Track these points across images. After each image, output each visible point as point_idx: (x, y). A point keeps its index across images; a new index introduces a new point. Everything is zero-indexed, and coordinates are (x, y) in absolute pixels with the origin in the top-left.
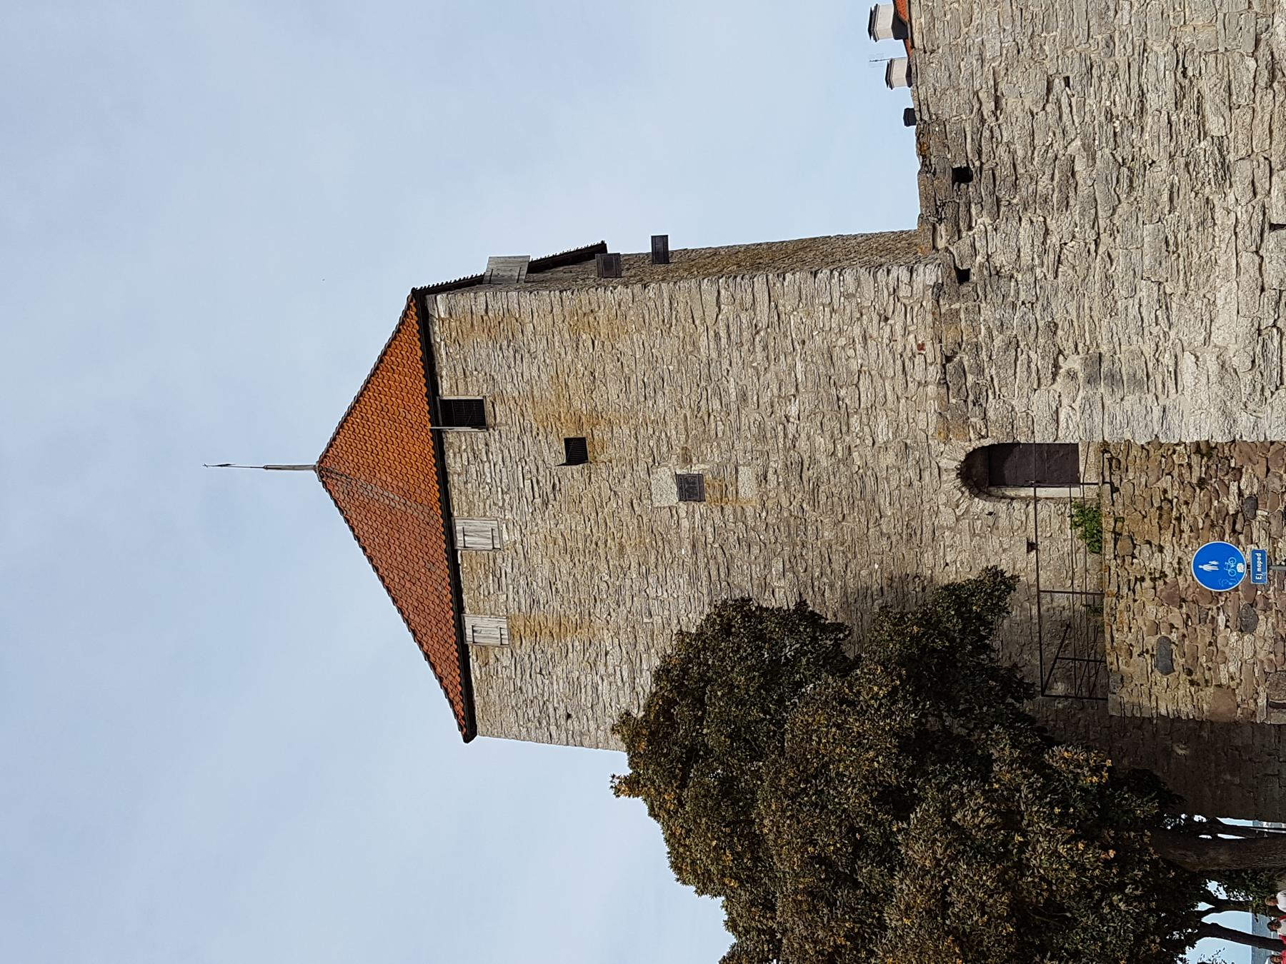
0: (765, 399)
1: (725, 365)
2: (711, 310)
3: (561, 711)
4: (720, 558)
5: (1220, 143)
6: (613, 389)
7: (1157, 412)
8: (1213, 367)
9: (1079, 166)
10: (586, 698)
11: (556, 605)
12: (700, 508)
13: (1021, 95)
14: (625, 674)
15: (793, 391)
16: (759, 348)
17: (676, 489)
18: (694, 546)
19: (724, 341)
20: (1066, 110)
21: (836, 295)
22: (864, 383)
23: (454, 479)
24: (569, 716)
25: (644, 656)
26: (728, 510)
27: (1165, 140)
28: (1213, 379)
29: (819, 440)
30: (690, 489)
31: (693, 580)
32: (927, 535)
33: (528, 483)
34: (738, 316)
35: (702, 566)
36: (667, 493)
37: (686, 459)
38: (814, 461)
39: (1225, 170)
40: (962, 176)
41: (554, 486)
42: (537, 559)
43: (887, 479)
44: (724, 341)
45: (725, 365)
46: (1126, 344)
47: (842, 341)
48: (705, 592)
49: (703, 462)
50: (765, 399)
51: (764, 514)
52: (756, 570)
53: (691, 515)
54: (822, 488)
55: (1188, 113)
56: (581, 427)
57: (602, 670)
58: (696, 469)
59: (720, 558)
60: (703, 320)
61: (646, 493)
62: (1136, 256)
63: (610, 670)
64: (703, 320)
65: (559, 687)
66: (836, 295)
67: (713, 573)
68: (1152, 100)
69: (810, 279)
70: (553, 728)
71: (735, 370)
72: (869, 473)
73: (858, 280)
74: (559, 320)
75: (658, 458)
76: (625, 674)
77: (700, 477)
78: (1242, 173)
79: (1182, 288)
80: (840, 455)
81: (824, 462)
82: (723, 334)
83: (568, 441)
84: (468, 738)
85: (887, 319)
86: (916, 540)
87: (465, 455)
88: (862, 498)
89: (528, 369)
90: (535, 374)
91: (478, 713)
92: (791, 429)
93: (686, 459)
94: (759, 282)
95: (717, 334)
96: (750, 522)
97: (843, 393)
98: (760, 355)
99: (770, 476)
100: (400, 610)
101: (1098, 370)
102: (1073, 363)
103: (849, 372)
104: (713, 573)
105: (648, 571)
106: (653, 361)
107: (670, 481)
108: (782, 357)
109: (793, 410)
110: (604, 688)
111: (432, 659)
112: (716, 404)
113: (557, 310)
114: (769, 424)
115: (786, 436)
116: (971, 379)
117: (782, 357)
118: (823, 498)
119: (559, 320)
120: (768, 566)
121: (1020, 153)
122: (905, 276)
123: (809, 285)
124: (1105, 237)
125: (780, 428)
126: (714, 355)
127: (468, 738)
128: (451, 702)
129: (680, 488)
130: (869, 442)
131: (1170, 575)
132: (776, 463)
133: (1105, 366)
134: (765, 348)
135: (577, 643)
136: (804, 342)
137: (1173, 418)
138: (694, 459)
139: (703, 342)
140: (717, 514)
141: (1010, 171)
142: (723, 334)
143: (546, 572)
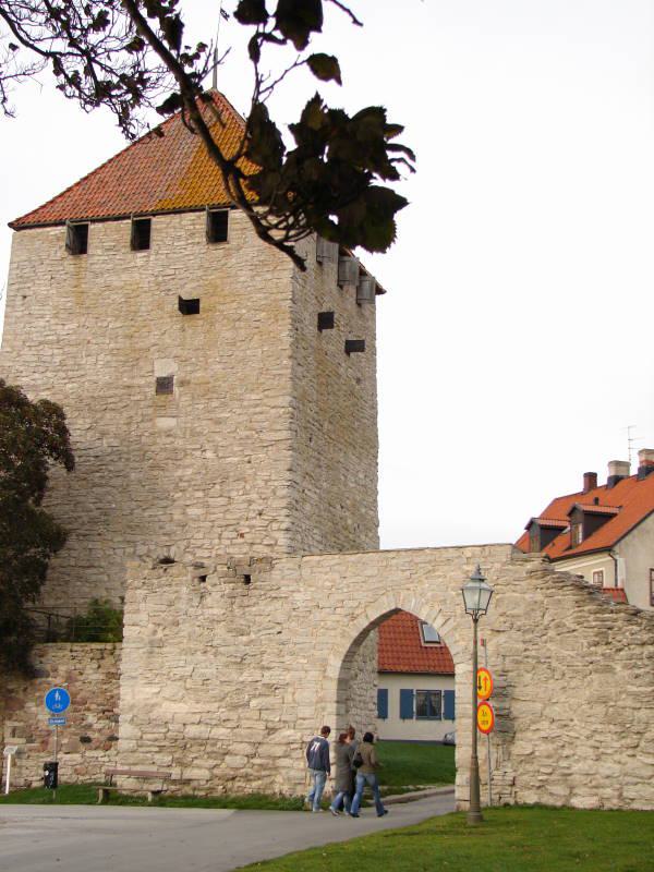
0: (218, 438)
1: (239, 411)
2: (273, 402)
3: (27, 293)
4: (120, 405)
5: (247, 705)
6: (228, 335)
7: (134, 674)
8: (153, 702)
9: (245, 638)
10: (35, 309)
11: (94, 291)
12: (152, 390)
13: (278, 610)
14: (51, 338)
15: (220, 455)
16: (248, 433)
17: (164, 375)
18: (129, 387)
19: (252, 410)
20: (269, 631)
21: (276, 483)
22: (222, 501)
23: (176, 219)
24: (25, 297)
25: (61, 351)
26: (150, 411)
27: (250, 679)
28: (148, 702)
29: (189, 472)
30: (164, 385)
31: (109, 385)
32: (129, 537)
33: (172, 272)
34: (267, 420)
35: (116, 392)
36: (162, 370)
37: (183, 383)
38: (179, 467)
39: (235, 707)
40: (247, 579)
41: (169, 290)
42: (124, 277)
43: (165, 514)
44: (252, 410)
45: (239, 411)
46: (171, 657)
47: (248, 487)
48: (101, 393)
49: (180, 395)
50: (218, 438)
51: (146, 434)
52: (113, 429)
53: (148, 385)
54: (161, 473)
55: (261, 690)
56: (204, 312)
57: (53, 321)
58: (176, 389)
59: (120, 405)
60: (267, 396)
61: (163, 355)
62: (203, 665)
63: (53, 328)
64: (267, 396)
65: (43, 290)
66: (276, 483)
67: (110, 400)
68: (267, 674)
69: (287, 467)
70: (17, 286)
71: (235, 417)
72: (169, 503)
73: (283, 498)
74: (273, 296)
75: (184, 364)
76: (51, 338)
77: (172, 392)
78: (233, 715)
79: (188, 686)
80: (180, 484)
81: (179, 473)
82: (258, 409)
83: (197, 302)
84: (10, 225)
85: (260, 514)
86: (129, 531)
87: (192, 227)
88: (154, 498)
89: (244, 276)
90: (242, 279)
91: (28, 231)
92: (198, 453)
93: (183, 383)
94: (285, 434)
95: (257, 405)
96: (141, 425)
97: (217, 487)
98: (244, 433)
99: (169, 440)
100: (104, 166)
101: (155, 646)
102: (160, 635)
103: (229, 491)
104: (110, 400)
105: (114, 355)
106: (244, 361)
107: (170, 371)
108: (241, 448)
109: (209, 454)
110: (42, 323)
111: (67, 194)
112: (215, 404)
113: (280, 296)
114: (202, 439)
115: (194, 450)
116: (155, 581)
117: (241, 448)
118: (155, 473)
119: (273, 296)
120: (116, 436)
121: (254, 609)
122: (284, 526)
123: (283, 466)
124: (214, 650)
125: (198, 446)
126: (245, 403)
127: (10, 225)
128: (35, 212)
129: (165, 378)
130: (188, 503)
131: (82, 678)
132: (179, 443)
133: (157, 650)
134: (248, 437)
135: (70, 304)
136: (249, 462)
137: (132, 682)
138: (182, 389)
139: (254, 397)
140: (147, 403)
141: (246, 604)
142: (258, 409)
143: (116, 284)
